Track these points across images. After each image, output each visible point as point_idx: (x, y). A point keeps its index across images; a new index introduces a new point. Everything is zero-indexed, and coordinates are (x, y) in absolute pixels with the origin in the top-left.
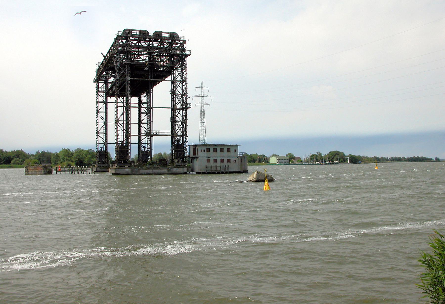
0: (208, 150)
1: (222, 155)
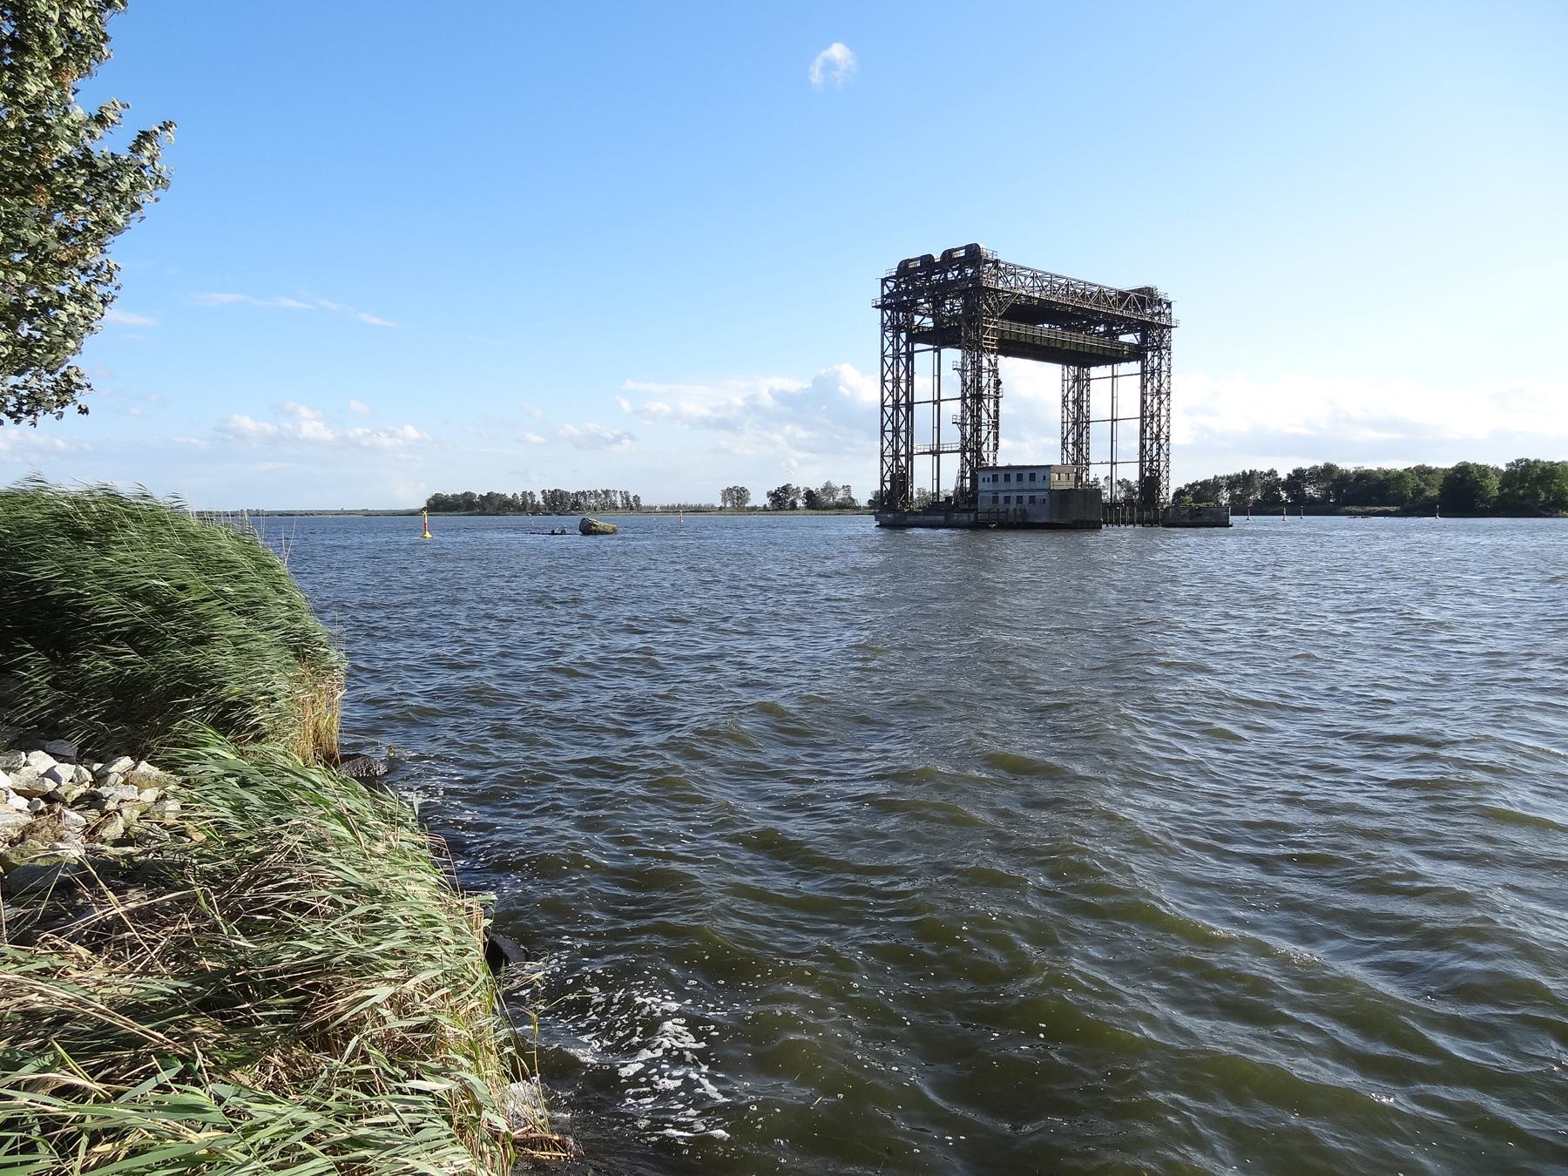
0: (995, 478)
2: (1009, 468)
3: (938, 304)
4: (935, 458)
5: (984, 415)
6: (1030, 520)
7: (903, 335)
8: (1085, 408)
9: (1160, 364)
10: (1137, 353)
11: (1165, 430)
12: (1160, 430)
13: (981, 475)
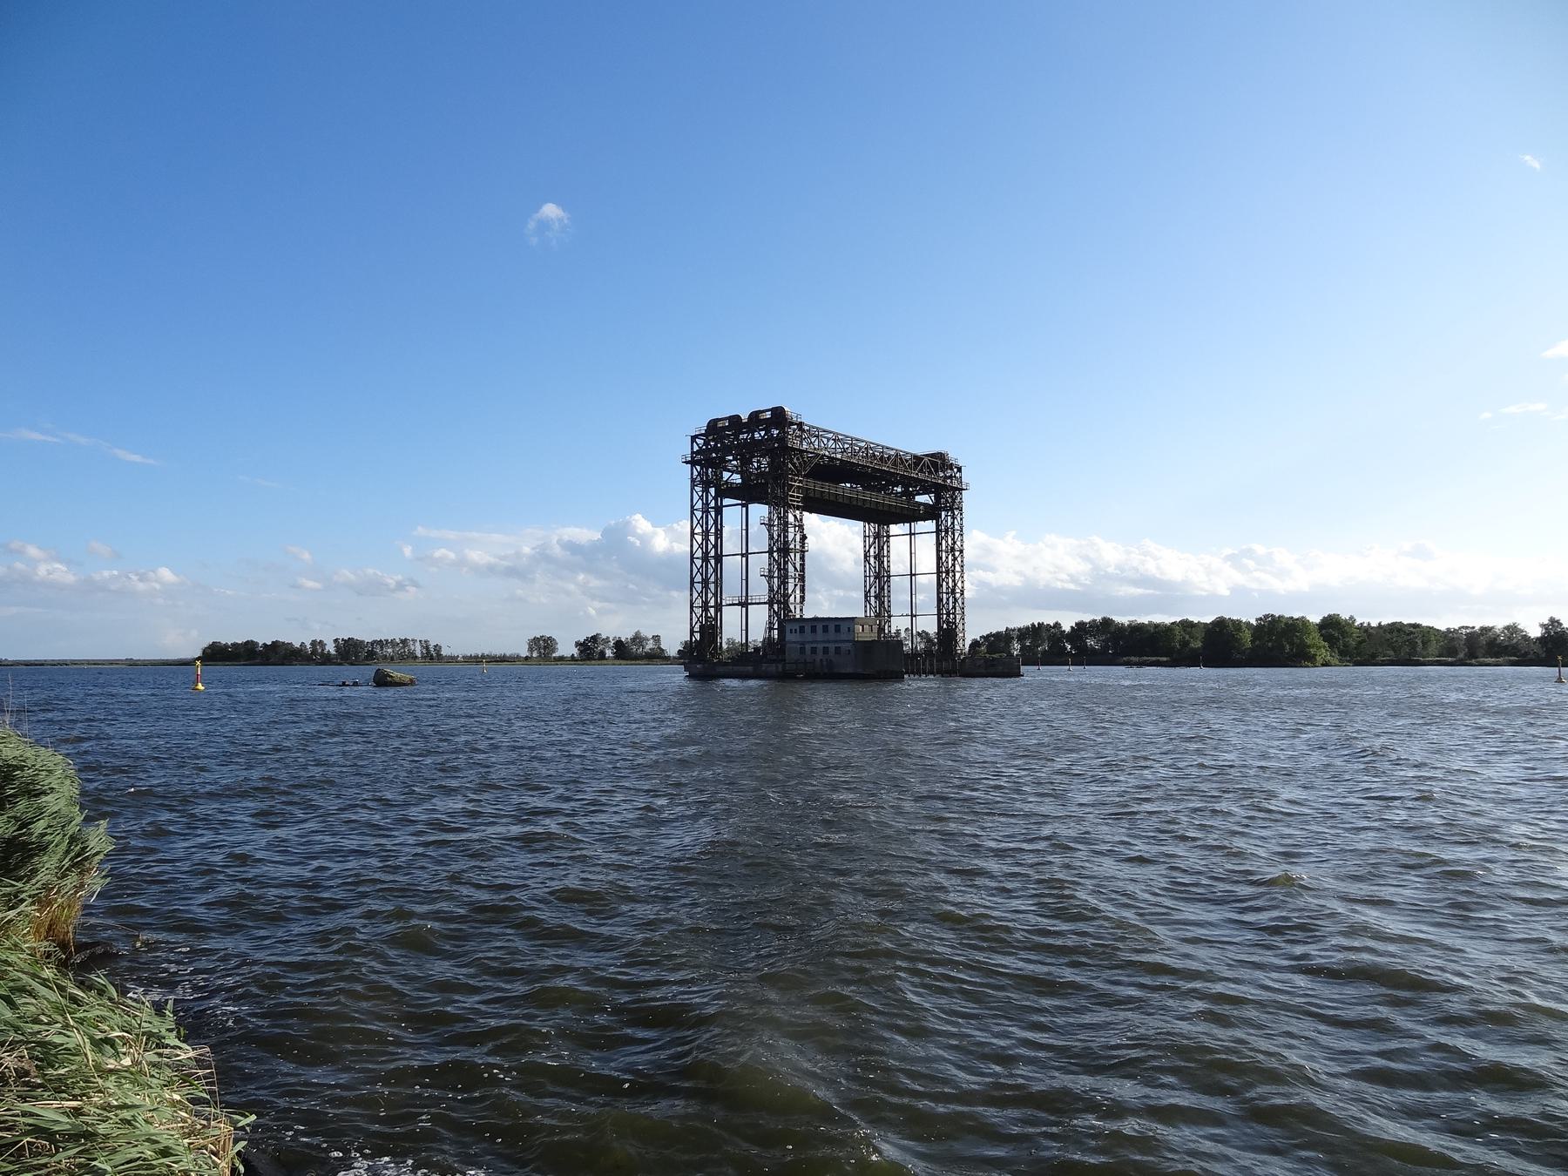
0: (802, 630)
2: (816, 619)
3: (745, 462)
4: (744, 609)
5: (791, 568)
7: (712, 490)
8: (885, 563)
9: (953, 523)
10: (931, 513)
11: (959, 584)
12: (955, 585)
13: (788, 627)
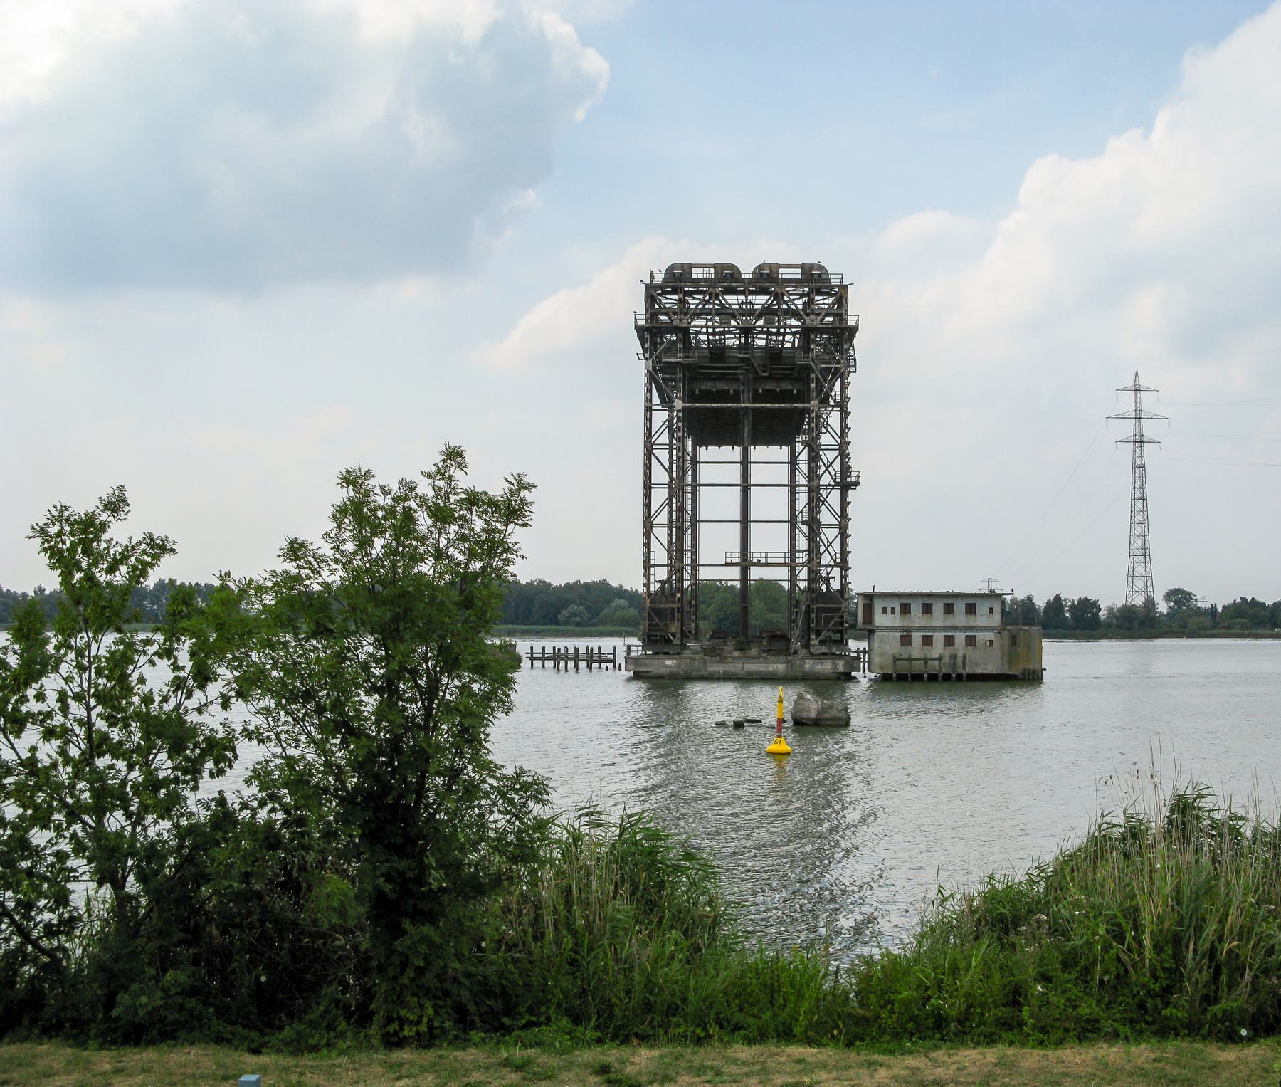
1: (948, 624)
6: (969, 670)
